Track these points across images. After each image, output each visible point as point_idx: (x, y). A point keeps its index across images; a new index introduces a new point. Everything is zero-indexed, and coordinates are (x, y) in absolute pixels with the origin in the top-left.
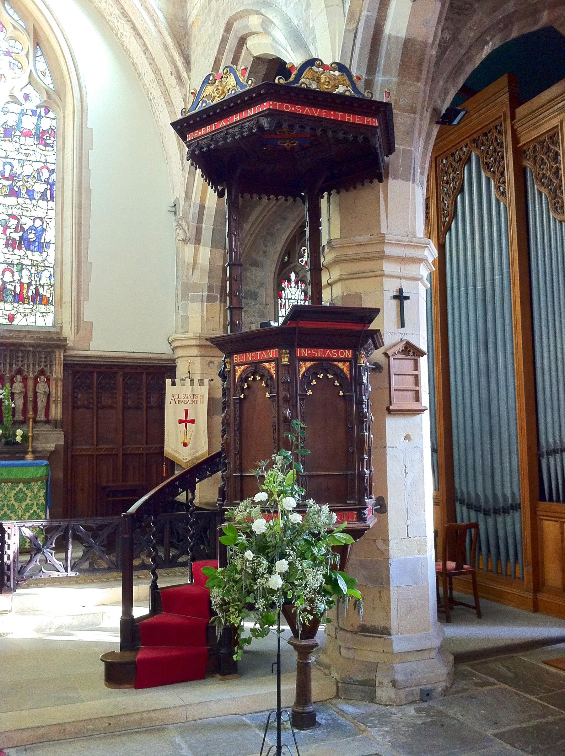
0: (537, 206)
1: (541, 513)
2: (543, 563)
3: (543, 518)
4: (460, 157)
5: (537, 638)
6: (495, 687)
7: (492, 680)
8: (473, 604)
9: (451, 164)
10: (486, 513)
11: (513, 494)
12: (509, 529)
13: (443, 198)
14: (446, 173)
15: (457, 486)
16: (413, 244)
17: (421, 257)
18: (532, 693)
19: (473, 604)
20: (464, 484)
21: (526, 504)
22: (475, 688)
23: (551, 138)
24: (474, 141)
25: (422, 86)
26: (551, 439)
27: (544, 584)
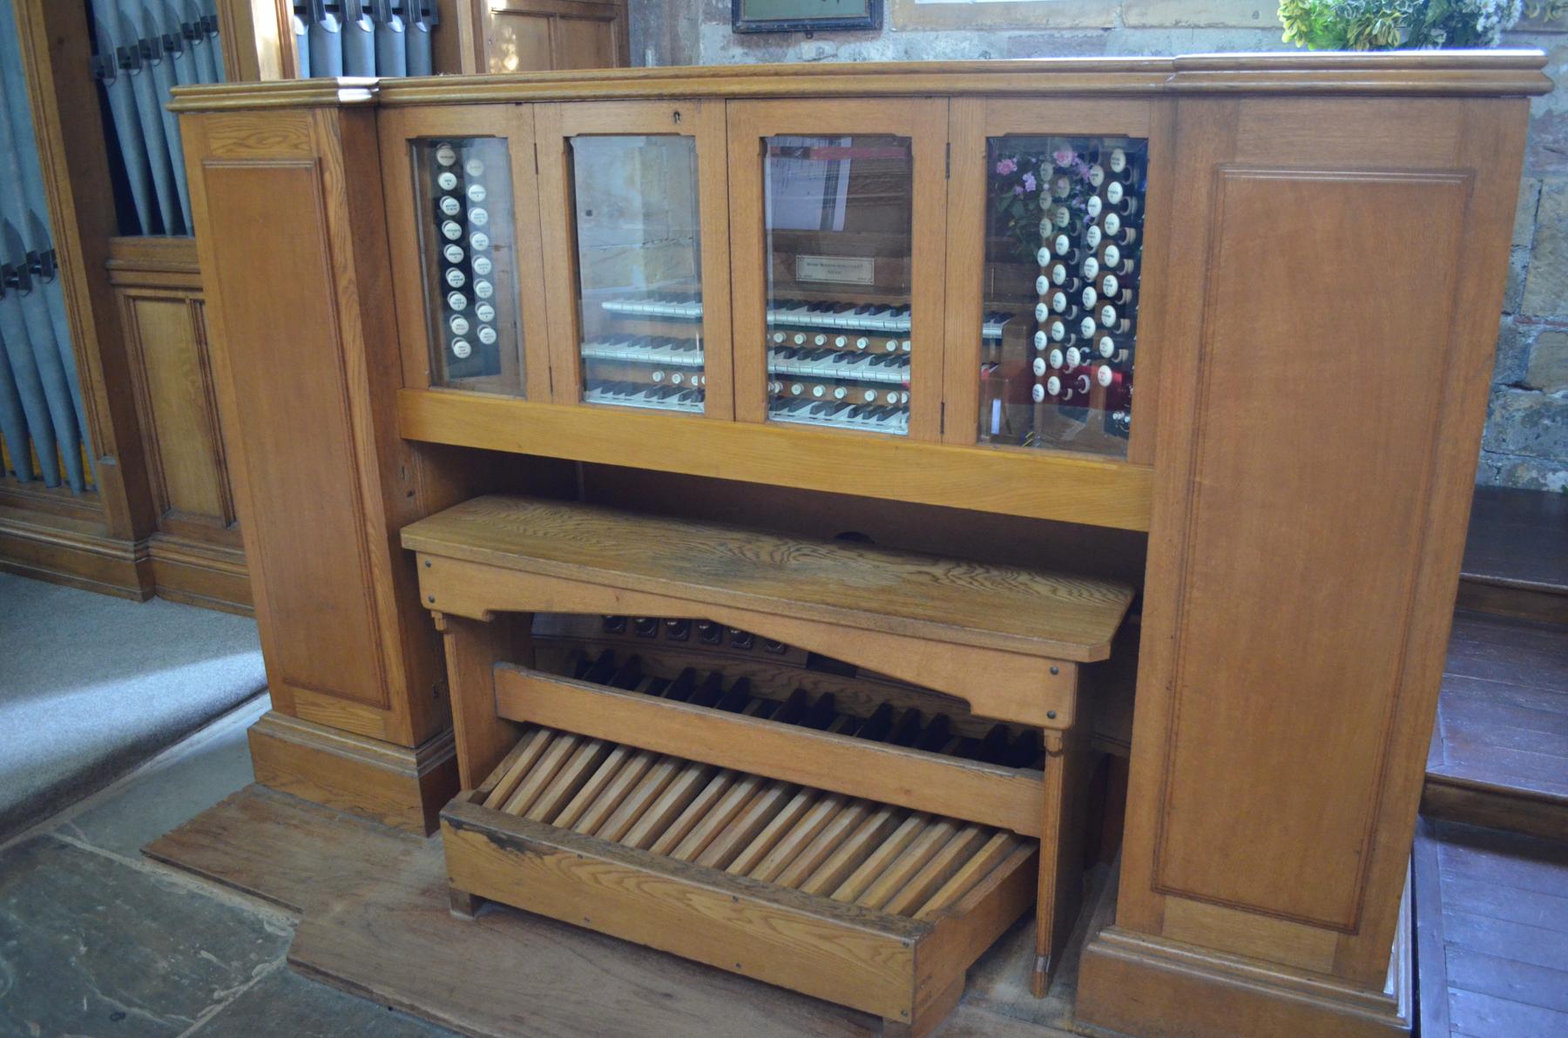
1: (130, 277)
3: (133, 292)
11: (34, 221)
12: (40, 336)
21: (68, 244)
27: (166, 506)
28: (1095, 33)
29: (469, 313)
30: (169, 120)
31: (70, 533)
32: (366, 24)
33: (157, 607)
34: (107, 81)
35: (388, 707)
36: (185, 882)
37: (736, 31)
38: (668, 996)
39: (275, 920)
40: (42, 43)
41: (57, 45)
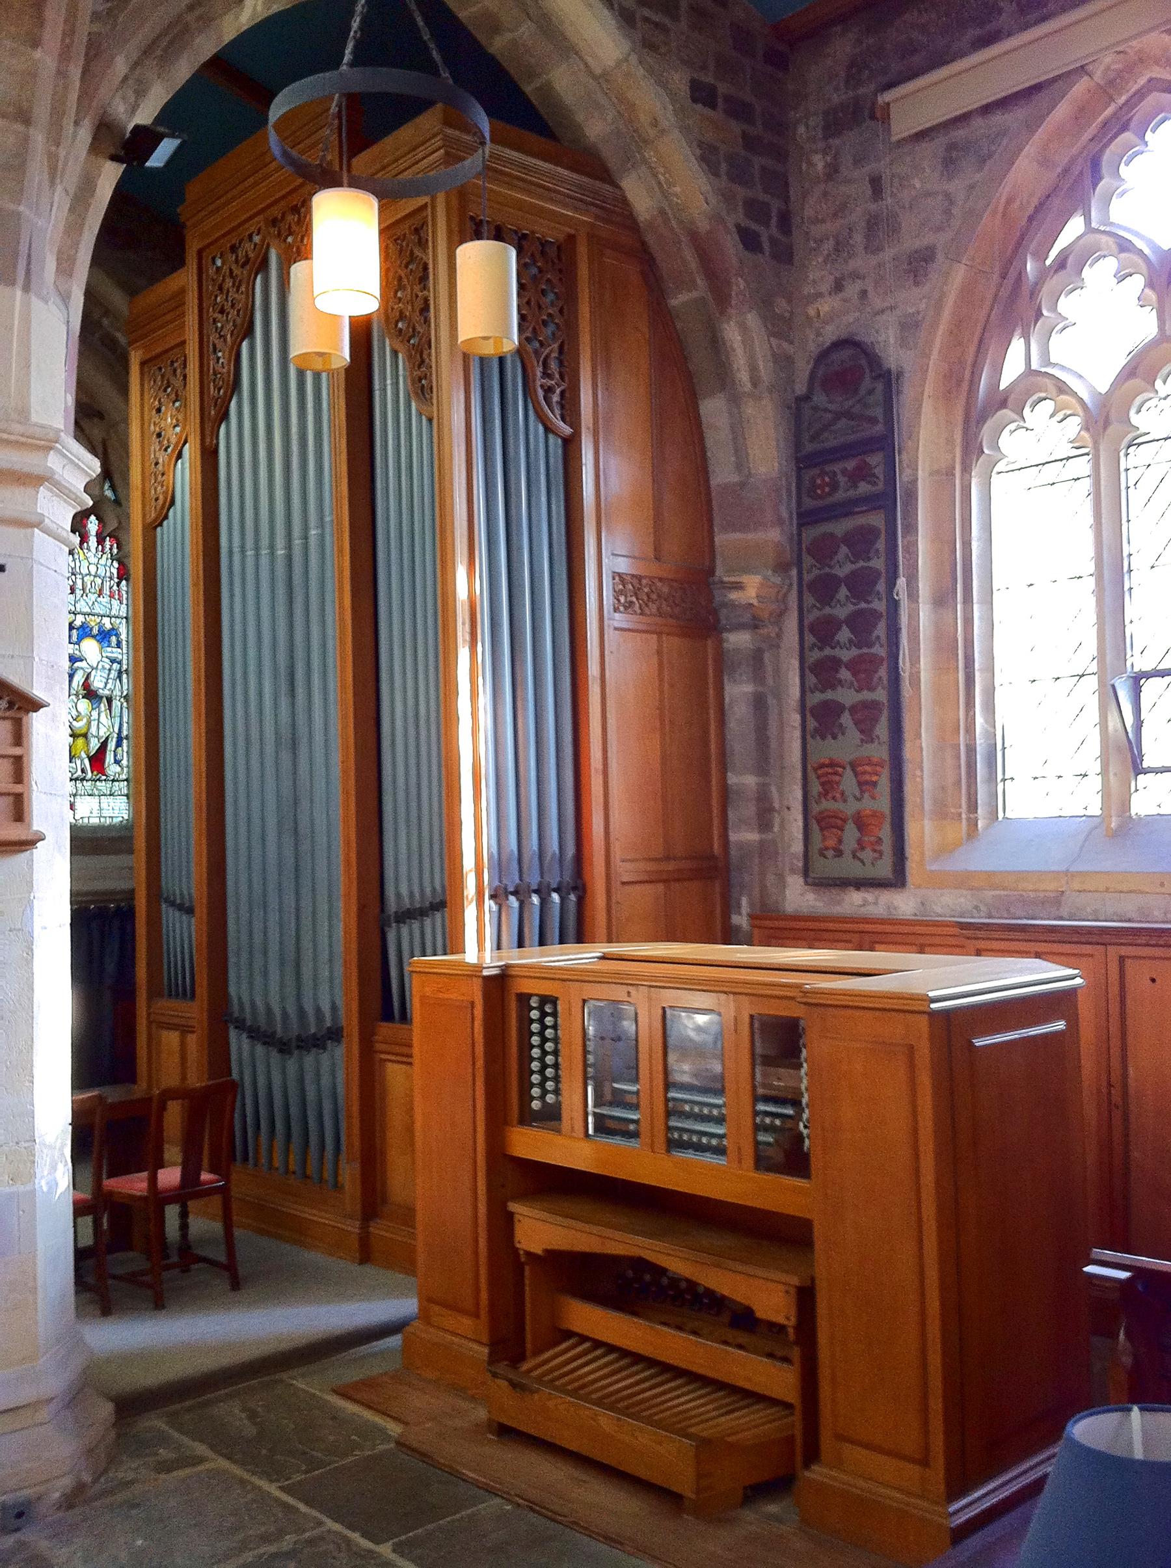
0: (389, 382)
1: (382, 1047)
2: (383, 1153)
3: (383, 1056)
4: (247, 256)
5: (338, 1332)
6: (207, 1466)
7: (201, 1449)
8: (223, 1259)
9: (231, 270)
10: (284, 1048)
11: (334, 1008)
12: (325, 1080)
13: (214, 346)
14: (221, 288)
15: (232, 990)
16: (12, 438)
17: (37, 471)
18: (274, 1472)
19: (223, 1259)
20: (245, 986)
22: (153, 1475)
23: (417, 231)
24: (274, 222)
25: (48, 60)
26: (404, 891)
27: (384, 1201)
28: (1052, 895)
29: (542, 1085)
30: (406, 974)
31: (323, 1214)
32: (535, 899)
33: (369, 1270)
34: (387, 929)
35: (477, 1316)
36: (351, 1407)
37: (806, 883)
38: (584, 1482)
39: (394, 1429)
40: (354, 908)
41: (362, 909)
